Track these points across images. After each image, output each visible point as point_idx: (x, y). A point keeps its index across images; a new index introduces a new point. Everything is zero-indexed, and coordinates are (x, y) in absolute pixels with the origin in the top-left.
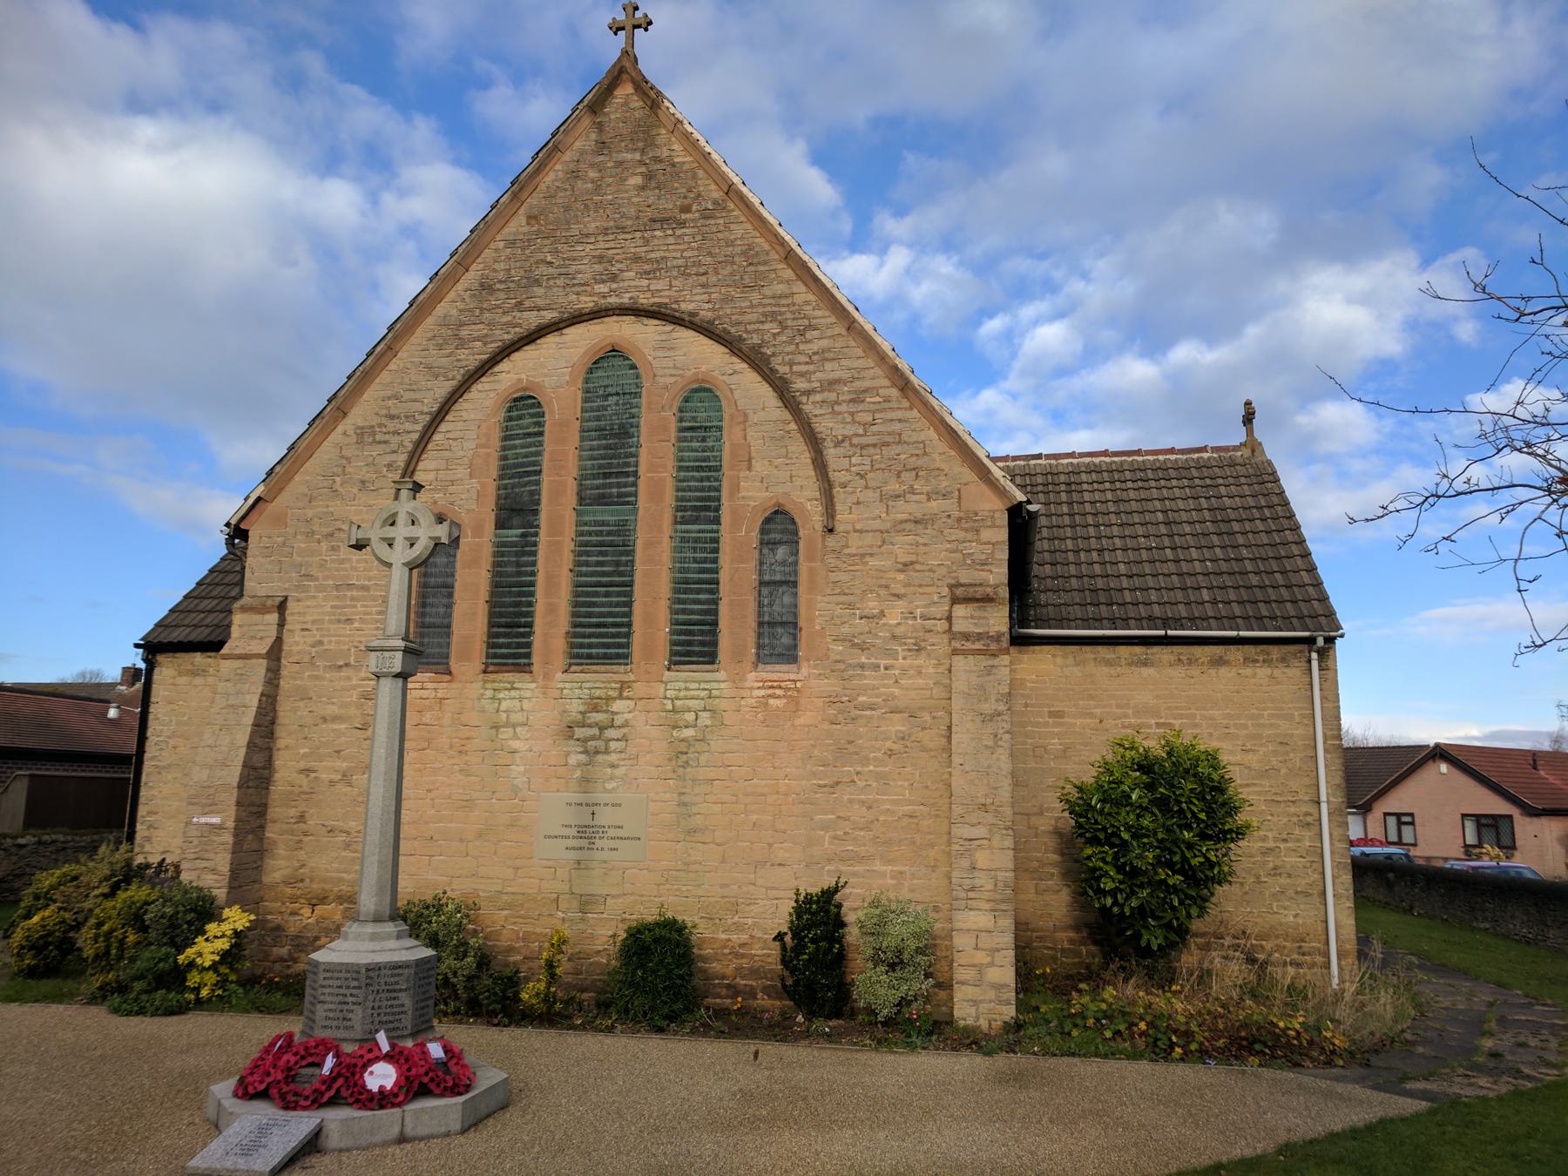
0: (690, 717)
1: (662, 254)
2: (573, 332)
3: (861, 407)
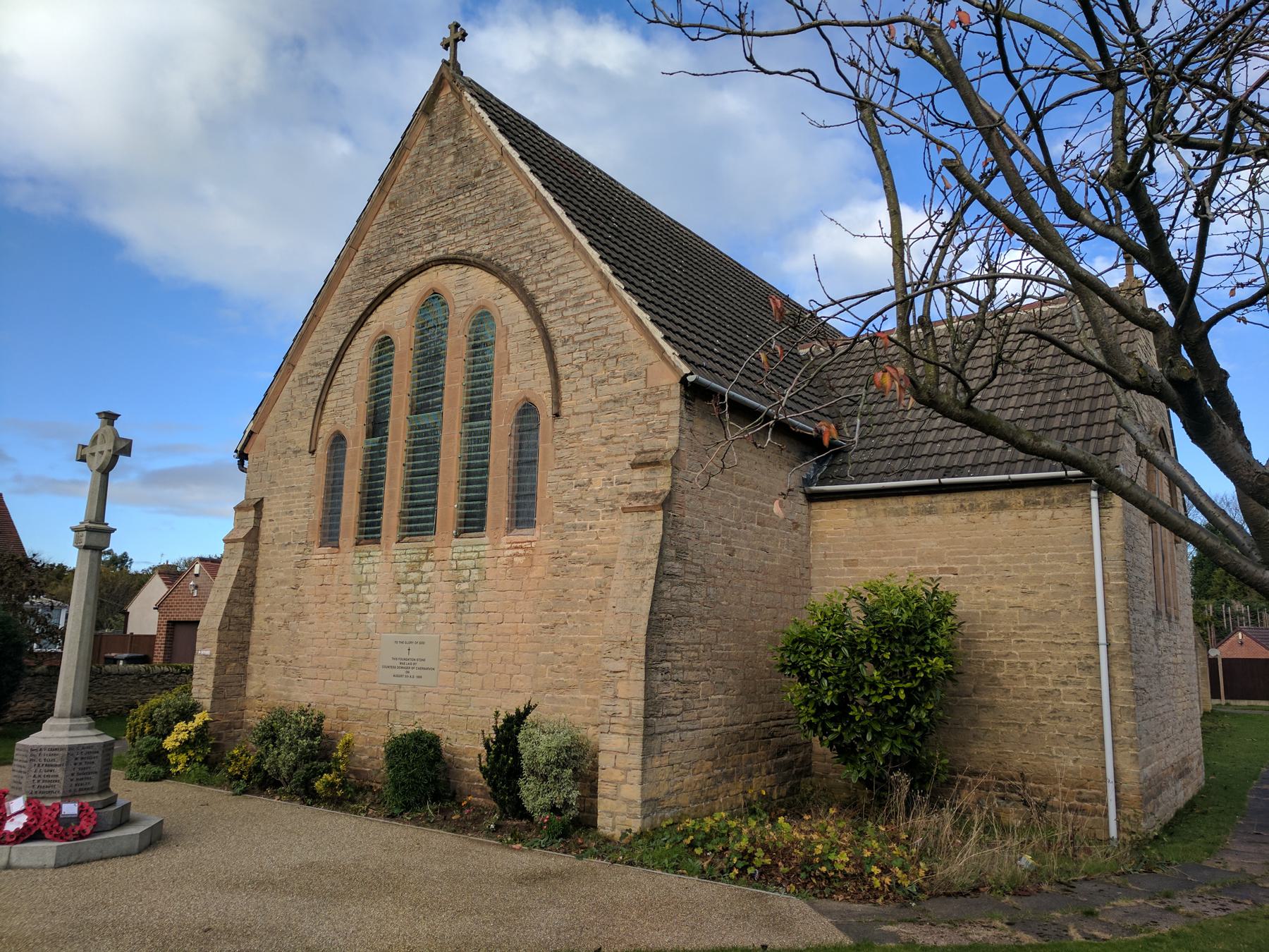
0: (466, 573)
1: (463, 212)
2: (411, 284)
3: (580, 310)
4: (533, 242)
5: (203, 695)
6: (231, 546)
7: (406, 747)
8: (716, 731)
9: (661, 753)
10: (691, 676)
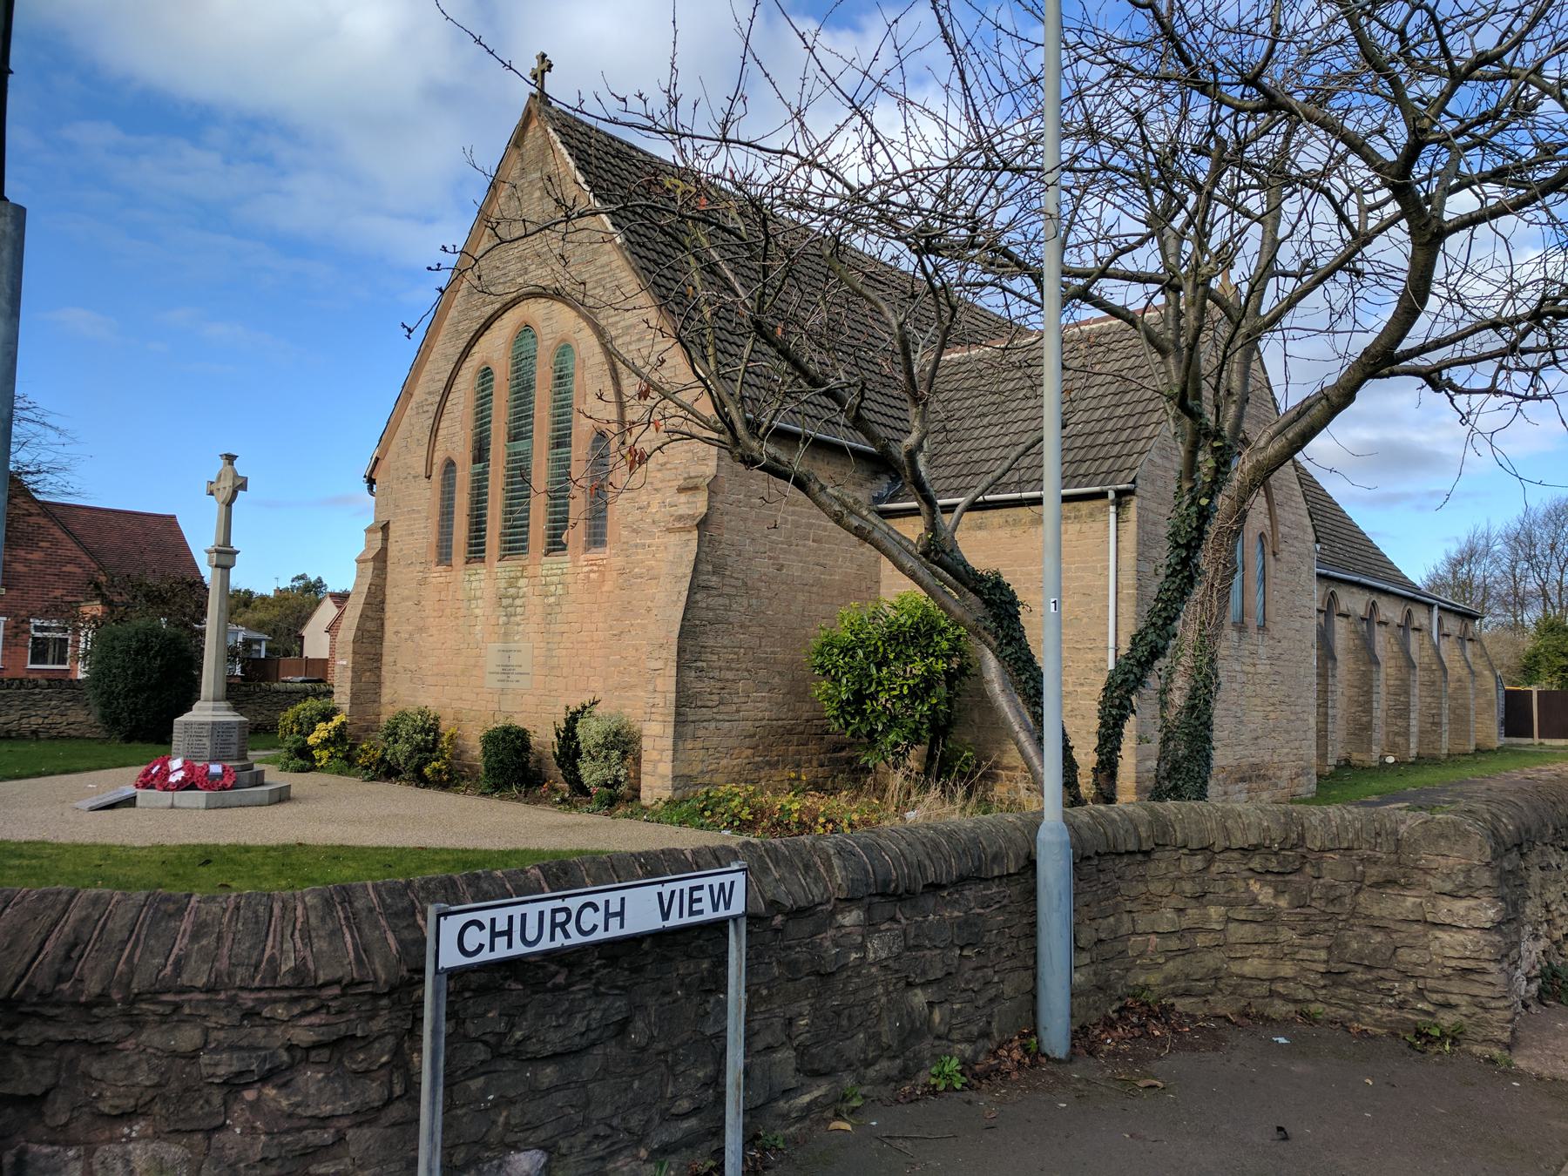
0: (553, 588)
4: (605, 279)
5: (343, 701)
6: (363, 565)
7: (496, 737)
8: (757, 724)
9: (695, 738)
10: (730, 675)
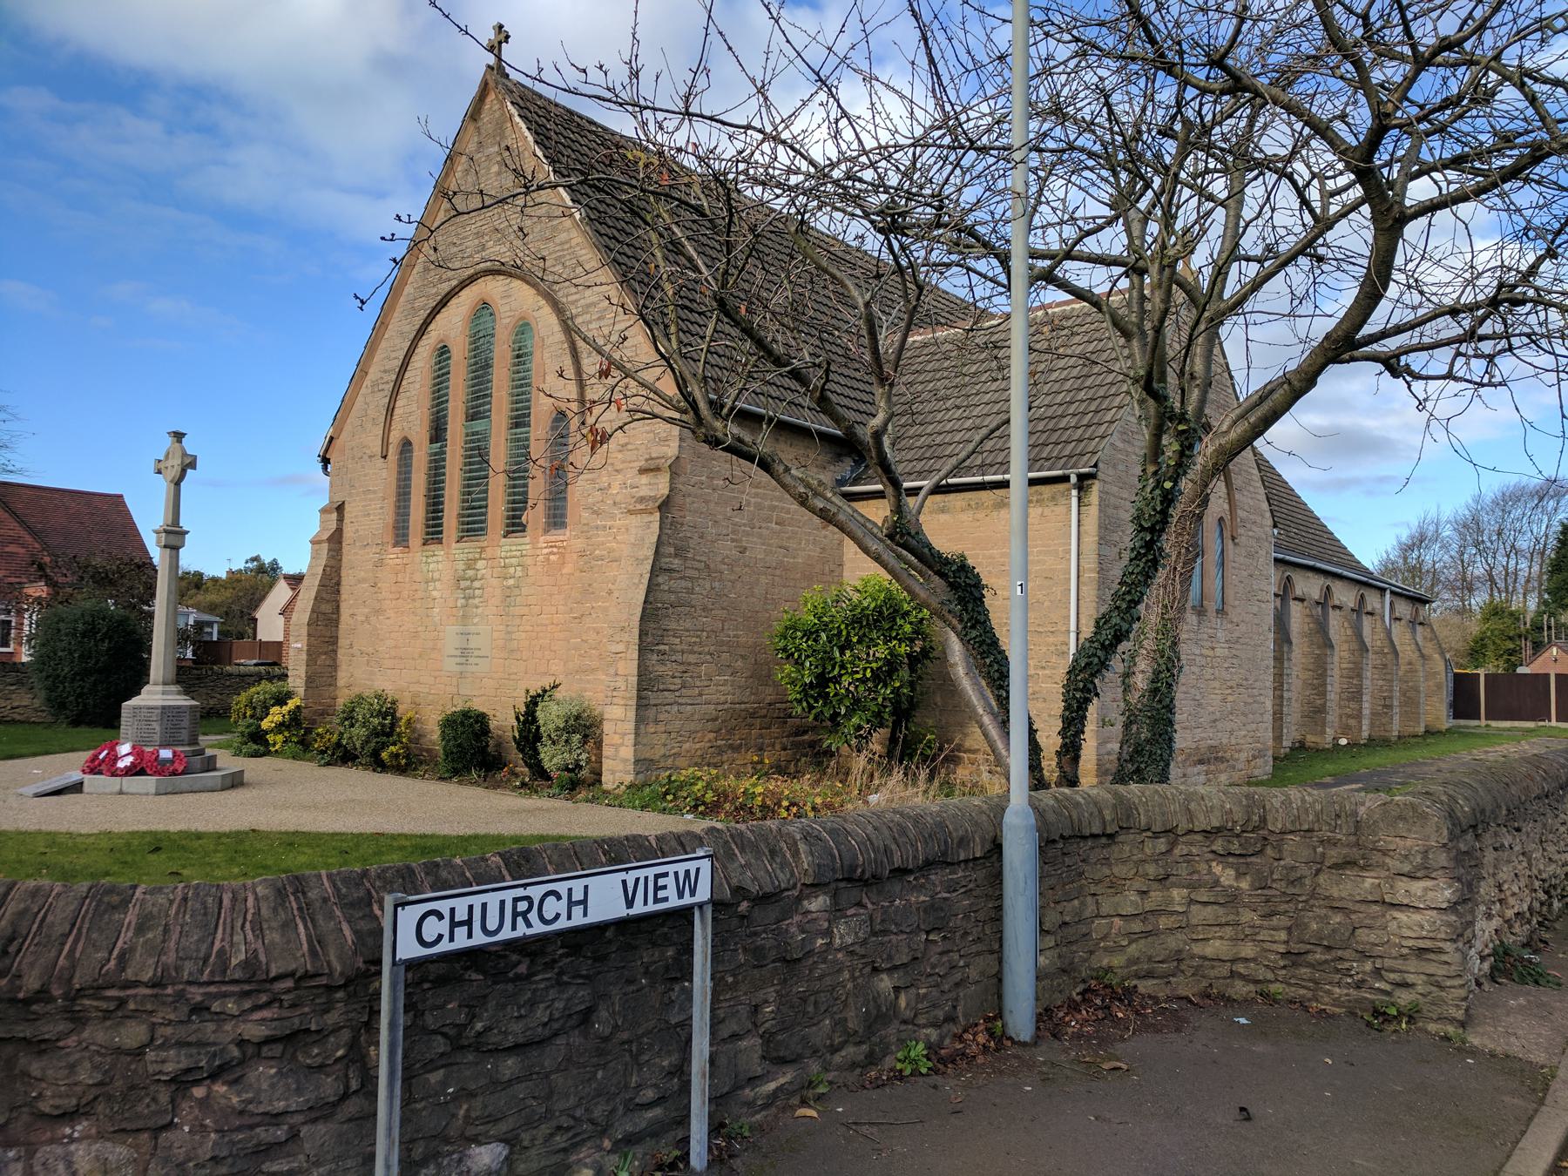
0: (512, 570)
5: (297, 684)
6: (317, 546)
7: (455, 722)
8: (720, 707)
9: (657, 722)
10: (692, 658)
